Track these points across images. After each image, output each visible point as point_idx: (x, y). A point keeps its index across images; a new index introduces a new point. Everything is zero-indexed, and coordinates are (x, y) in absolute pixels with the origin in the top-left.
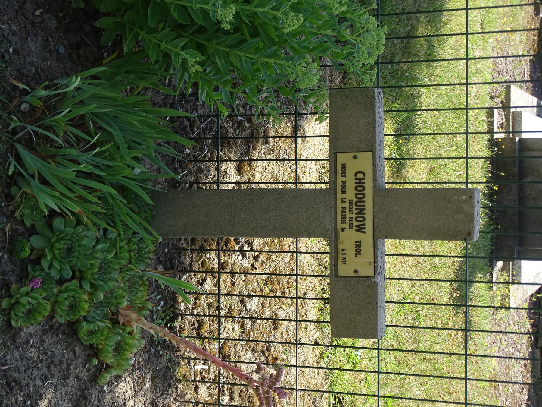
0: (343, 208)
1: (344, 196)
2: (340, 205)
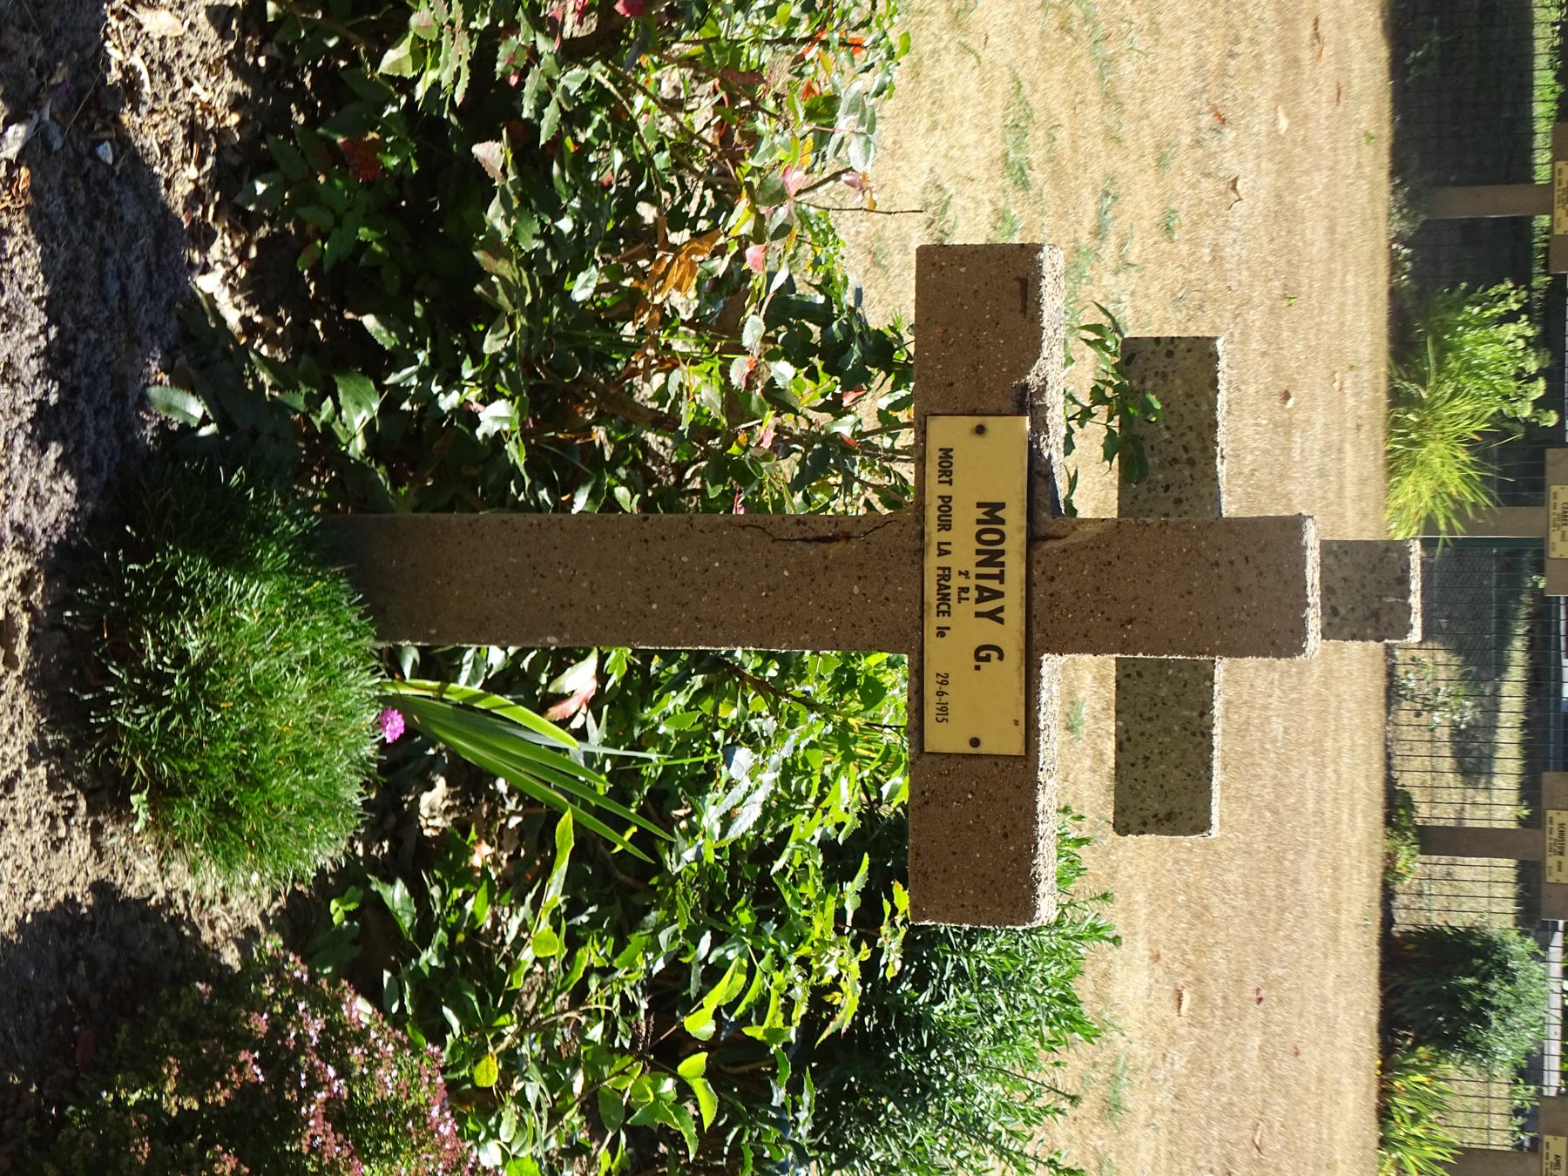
0: (944, 569)
1: (944, 536)
2: (932, 562)
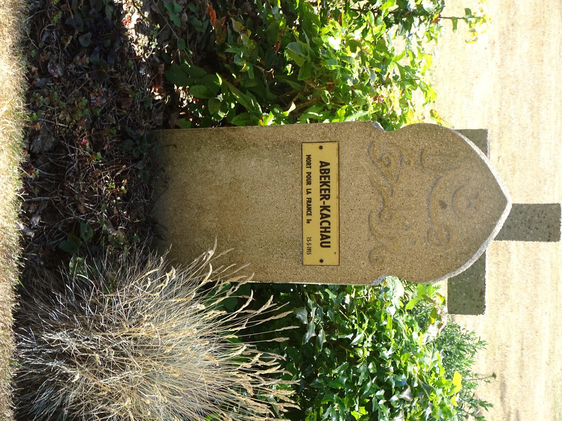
2: (305, 196)
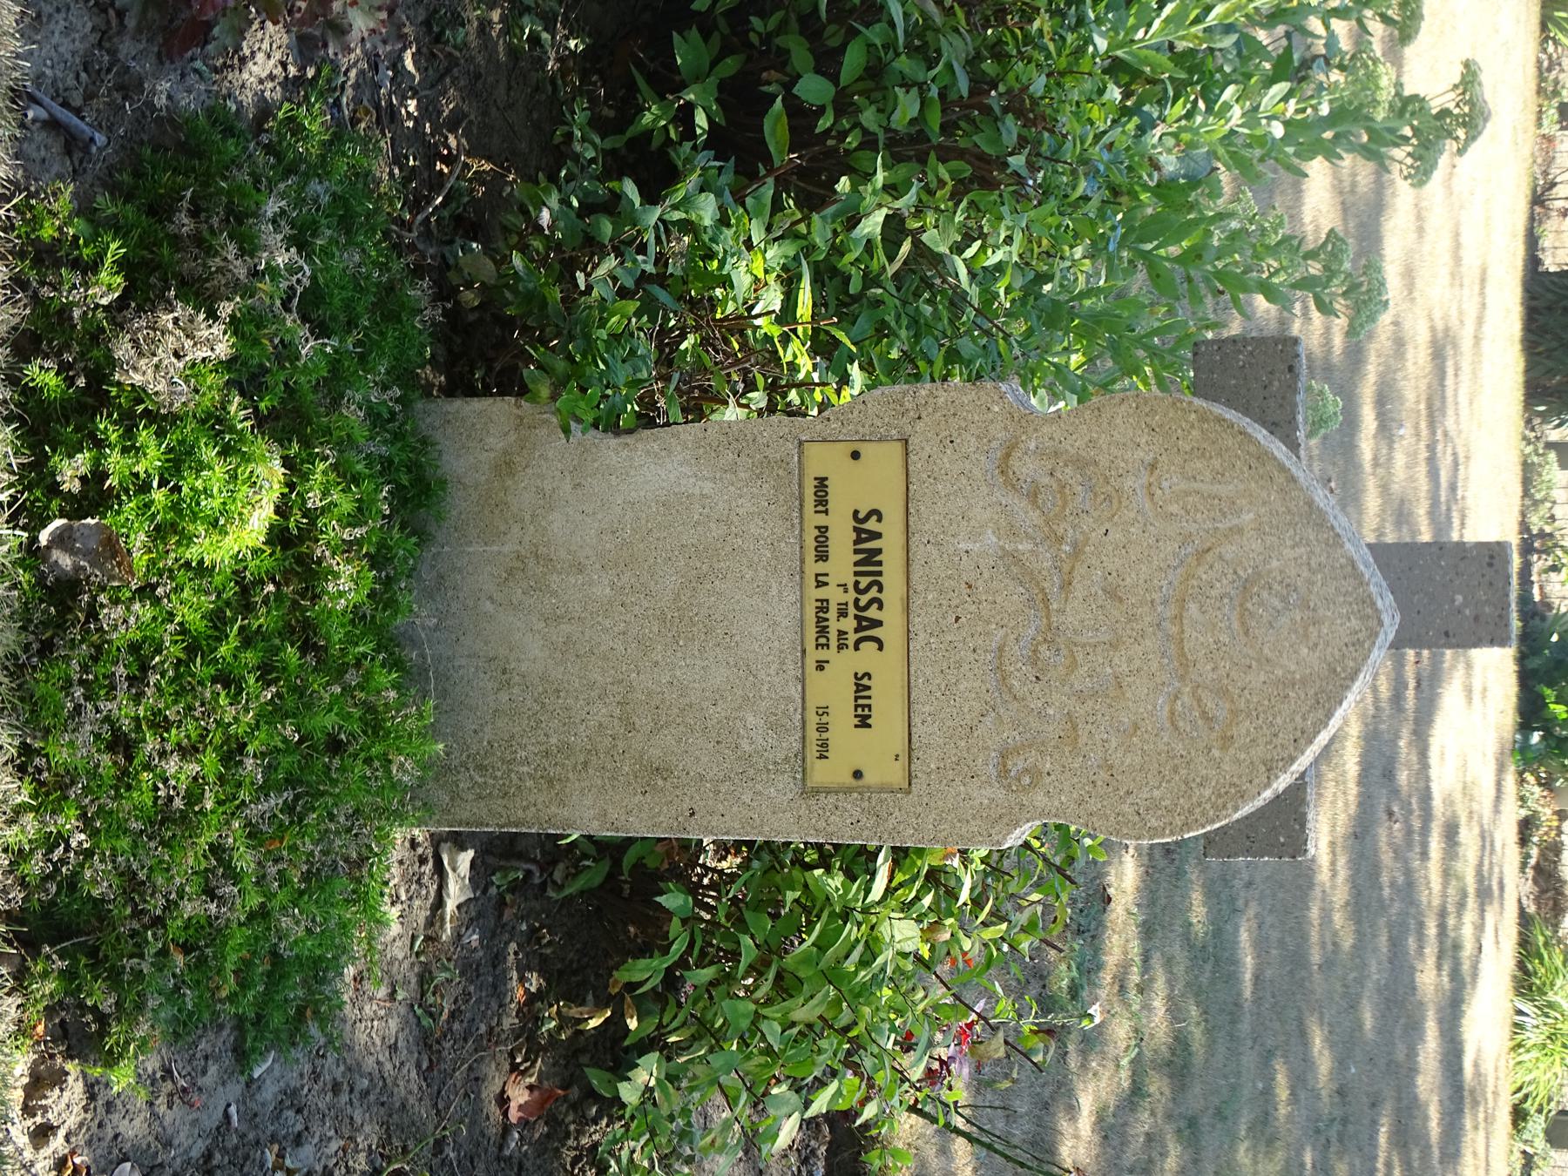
1: (821, 567)
